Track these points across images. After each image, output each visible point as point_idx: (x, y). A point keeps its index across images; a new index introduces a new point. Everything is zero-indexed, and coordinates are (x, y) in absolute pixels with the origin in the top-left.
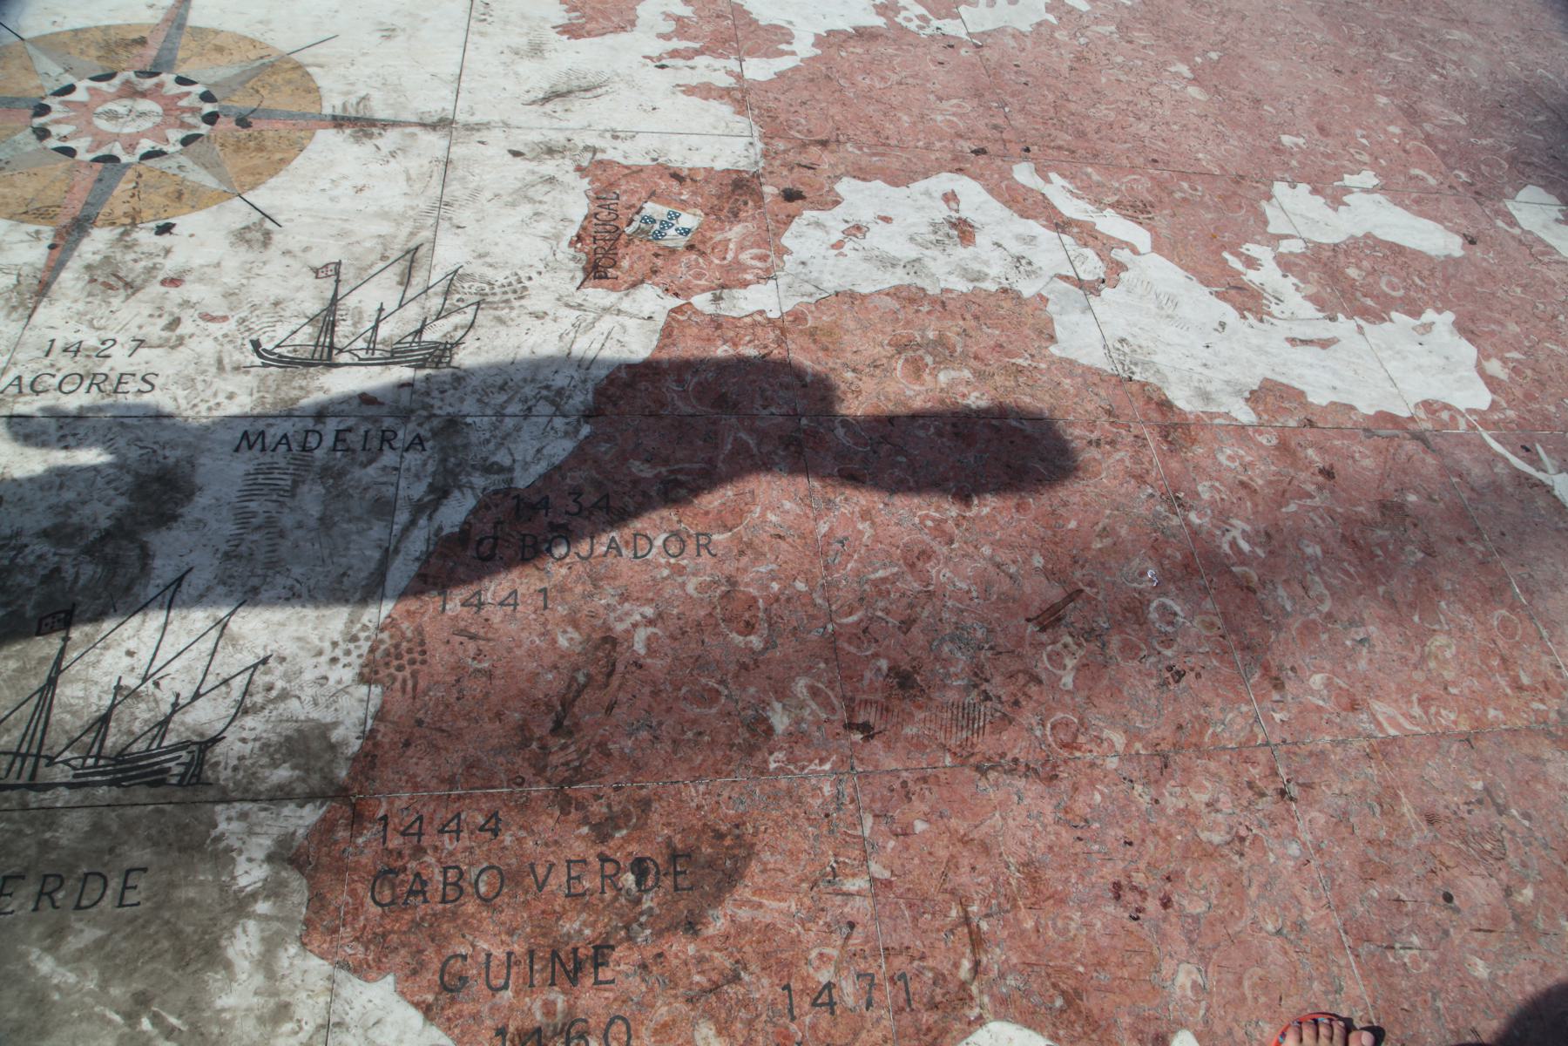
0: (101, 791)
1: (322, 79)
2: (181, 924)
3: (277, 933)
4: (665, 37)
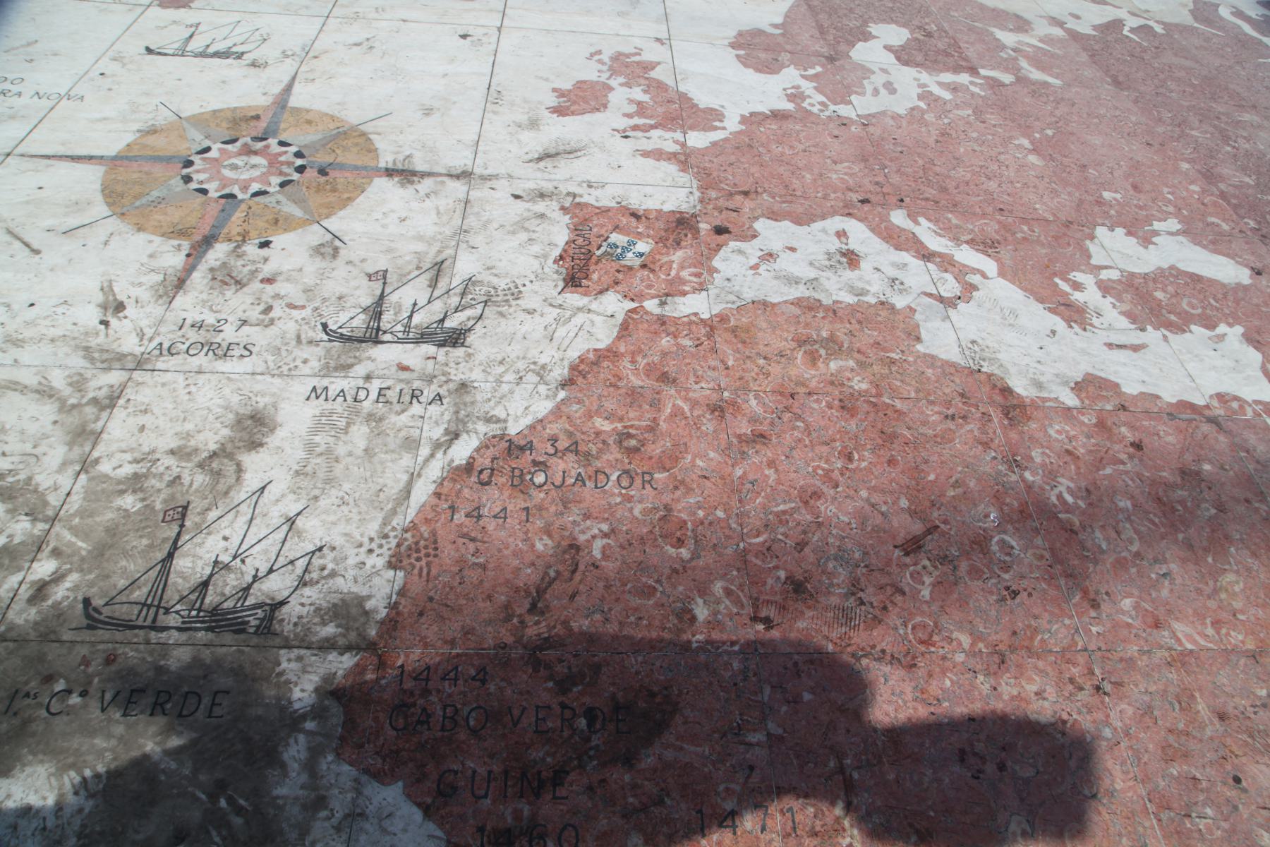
0: (200, 634)
1: (379, 142)
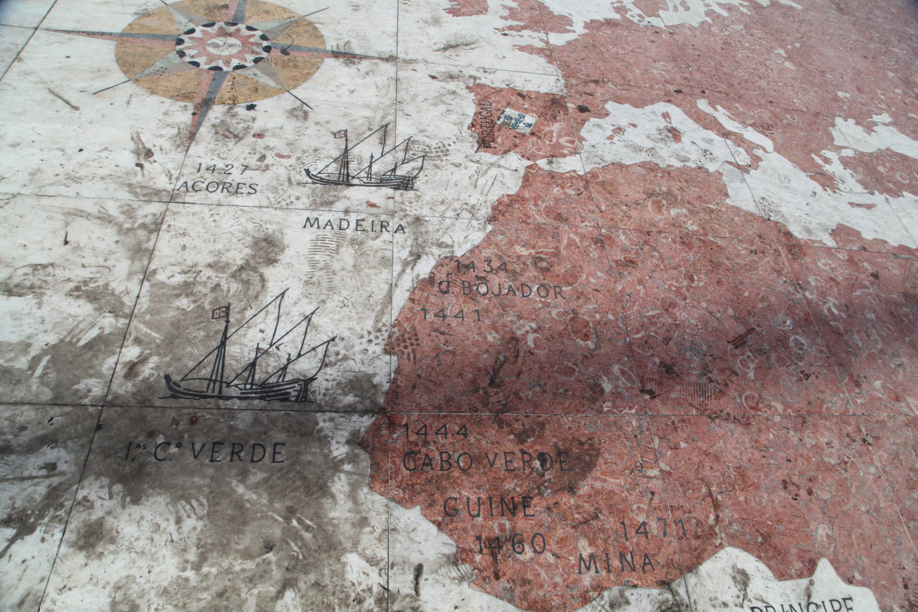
0: (256, 402)
1: (324, 31)
2: (306, 473)
3: (357, 481)
4: (503, 18)
